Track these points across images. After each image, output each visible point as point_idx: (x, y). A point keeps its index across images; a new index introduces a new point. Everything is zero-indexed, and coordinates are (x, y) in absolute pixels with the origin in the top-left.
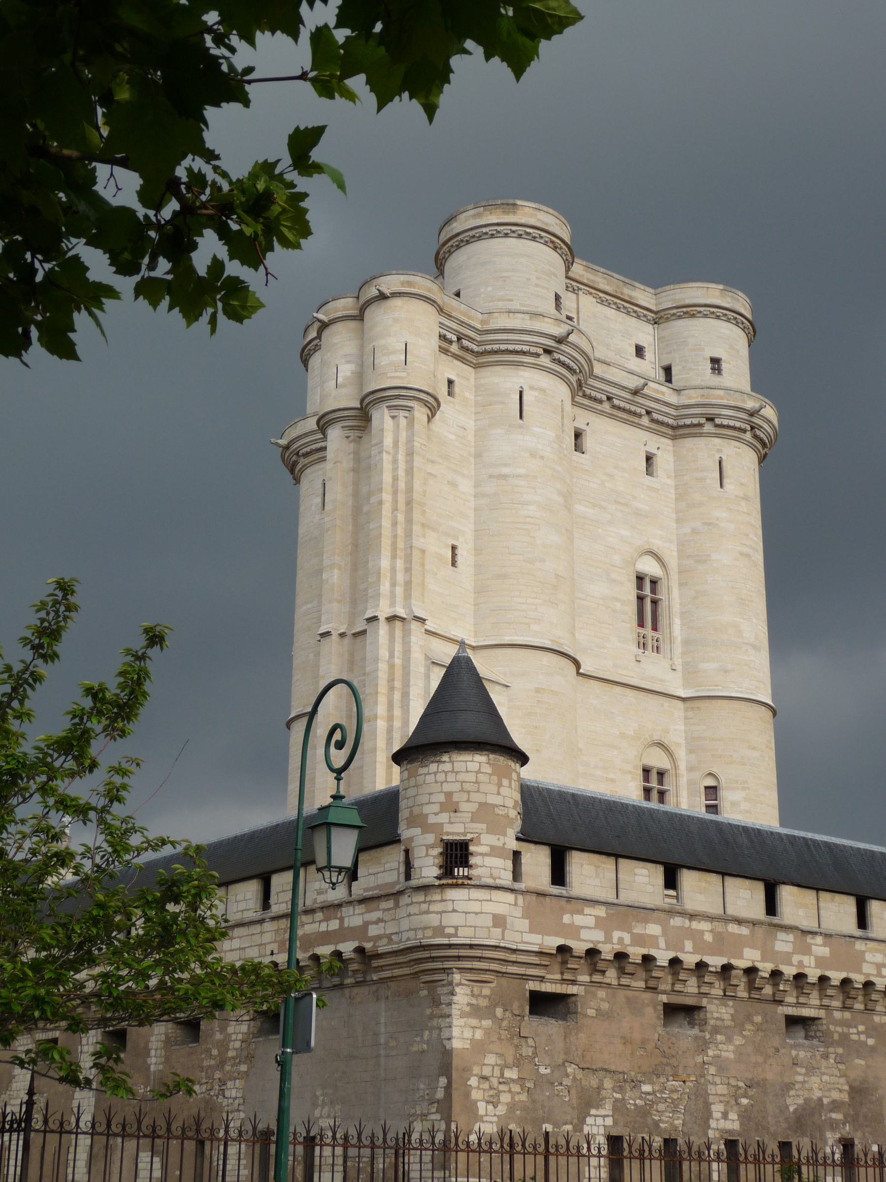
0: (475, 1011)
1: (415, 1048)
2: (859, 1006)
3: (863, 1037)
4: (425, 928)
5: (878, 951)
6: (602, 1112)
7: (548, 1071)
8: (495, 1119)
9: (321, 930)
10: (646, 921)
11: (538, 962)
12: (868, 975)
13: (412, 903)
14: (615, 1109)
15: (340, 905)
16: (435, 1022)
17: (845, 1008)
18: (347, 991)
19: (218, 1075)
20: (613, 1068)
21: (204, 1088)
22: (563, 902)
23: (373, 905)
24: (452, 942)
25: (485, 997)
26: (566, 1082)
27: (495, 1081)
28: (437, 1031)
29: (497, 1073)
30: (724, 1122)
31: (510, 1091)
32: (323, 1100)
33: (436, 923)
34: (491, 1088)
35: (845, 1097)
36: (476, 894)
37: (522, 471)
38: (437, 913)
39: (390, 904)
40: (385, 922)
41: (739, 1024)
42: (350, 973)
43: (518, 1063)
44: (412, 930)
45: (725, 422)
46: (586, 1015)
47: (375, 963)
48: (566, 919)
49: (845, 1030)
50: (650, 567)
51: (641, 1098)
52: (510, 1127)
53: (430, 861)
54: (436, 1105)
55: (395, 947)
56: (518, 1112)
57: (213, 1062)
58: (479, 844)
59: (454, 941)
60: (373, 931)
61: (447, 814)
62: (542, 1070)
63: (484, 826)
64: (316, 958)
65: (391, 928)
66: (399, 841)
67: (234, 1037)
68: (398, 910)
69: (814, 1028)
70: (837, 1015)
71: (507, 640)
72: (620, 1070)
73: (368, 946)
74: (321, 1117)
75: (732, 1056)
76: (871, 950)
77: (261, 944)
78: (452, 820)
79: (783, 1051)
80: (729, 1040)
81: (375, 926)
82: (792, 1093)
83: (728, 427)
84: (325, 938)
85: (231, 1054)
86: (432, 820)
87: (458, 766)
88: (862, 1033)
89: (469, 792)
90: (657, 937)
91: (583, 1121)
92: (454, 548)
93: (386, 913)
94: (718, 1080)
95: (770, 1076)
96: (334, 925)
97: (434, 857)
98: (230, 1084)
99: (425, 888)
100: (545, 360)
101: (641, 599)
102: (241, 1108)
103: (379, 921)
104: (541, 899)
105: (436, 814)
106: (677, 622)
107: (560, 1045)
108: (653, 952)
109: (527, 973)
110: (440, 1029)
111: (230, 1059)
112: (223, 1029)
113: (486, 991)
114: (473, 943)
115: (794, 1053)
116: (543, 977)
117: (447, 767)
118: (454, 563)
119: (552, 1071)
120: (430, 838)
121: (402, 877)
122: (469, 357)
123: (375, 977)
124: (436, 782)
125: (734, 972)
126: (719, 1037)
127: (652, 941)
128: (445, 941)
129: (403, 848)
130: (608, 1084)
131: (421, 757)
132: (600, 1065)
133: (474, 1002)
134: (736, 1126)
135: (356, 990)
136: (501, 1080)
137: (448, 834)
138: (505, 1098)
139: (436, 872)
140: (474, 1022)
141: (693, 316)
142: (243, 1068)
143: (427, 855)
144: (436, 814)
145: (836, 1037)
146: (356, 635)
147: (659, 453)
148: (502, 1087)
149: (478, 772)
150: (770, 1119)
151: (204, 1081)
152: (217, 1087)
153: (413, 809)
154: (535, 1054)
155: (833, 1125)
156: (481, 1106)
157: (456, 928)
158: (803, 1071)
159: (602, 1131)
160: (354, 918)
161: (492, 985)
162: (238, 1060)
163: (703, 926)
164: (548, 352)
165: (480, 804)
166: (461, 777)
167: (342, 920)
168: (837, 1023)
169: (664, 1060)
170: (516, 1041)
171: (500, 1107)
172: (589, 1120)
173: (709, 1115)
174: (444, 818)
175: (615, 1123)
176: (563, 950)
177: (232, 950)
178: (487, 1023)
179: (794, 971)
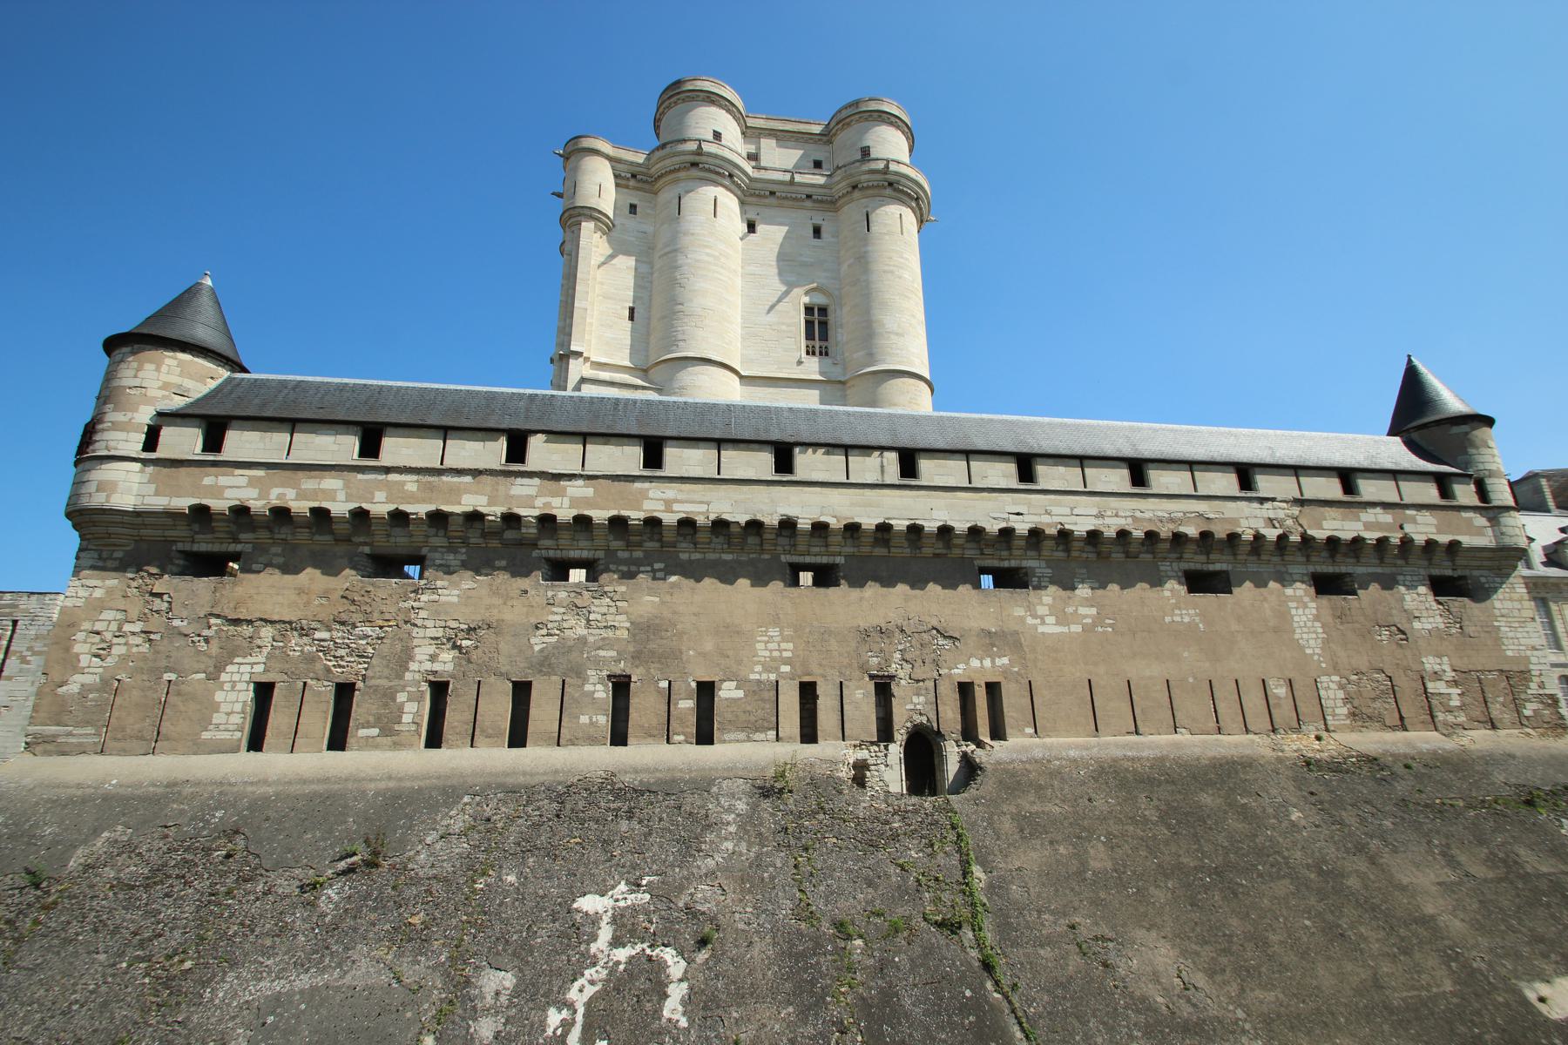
6: (250, 659)
10: (322, 478)
14: (269, 657)
20: (276, 618)
29: (114, 626)
34: (103, 641)
43: (142, 618)
48: (207, 481)
50: (820, 300)
62: (176, 623)
70: (622, 555)
82: (544, 632)
83: (868, 187)
90: (335, 491)
91: (220, 668)
94: (429, 623)
100: (694, 172)
101: (809, 324)
108: (325, 505)
115: (550, 594)
122: (646, 186)
127: (331, 495)
132: (258, 615)
134: (450, 667)
141: (848, 124)
148: (116, 640)
155: (598, 663)
156: (84, 660)
164: (695, 165)
169: (353, 608)
173: (411, 658)
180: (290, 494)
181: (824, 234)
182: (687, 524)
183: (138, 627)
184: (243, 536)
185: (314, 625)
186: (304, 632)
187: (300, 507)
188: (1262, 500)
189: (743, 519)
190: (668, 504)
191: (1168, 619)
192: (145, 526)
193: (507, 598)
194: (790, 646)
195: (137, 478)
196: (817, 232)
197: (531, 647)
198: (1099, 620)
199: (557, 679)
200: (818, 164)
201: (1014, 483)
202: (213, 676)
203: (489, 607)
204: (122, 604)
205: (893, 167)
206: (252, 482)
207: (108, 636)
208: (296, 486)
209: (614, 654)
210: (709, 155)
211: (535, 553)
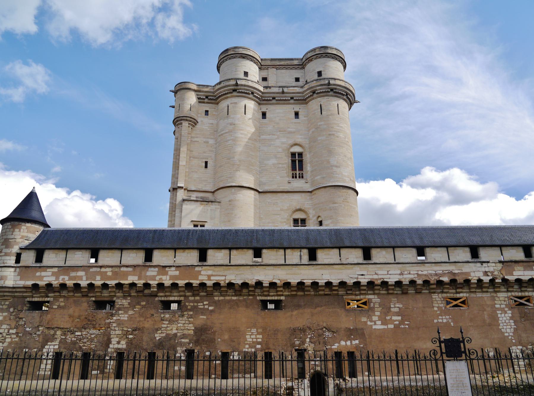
3: (206, 307)
5: (209, 270)
6: (53, 343)
10: (77, 271)
14: (60, 342)
17: (194, 295)
20: (62, 327)
26: (38, 333)
29: (6, 331)
31: (11, 338)
34: (2, 337)
37: (227, 131)
41: (132, 306)
43: (16, 327)
45: (319, 91)
48: (38, 274)
49: (195, 304)
51: (75, 337)
62: (28, 329)
70: (191, 298)
71: (221, 186)
72: (65, 327)
76: (205, 270)
80: (126, 312)
82: (160, 332)
83: (320, 93)
88: (206, 305)
90: (82, 276)
91: (43, 347)
92: (206, 163)
94: (117, 329)
100: (235, 94)
101: (293, 162)
104: (27, 268)
106: (309, 165)
107: (37, 319)
108: (79, 282)
113: (7, 303)
115: (162, 316)
118: (206, 167)
125: (124, 286)
126: (120, 312)
127: (81, 278)
130: (59, 333)
132: (55, 326)
134: (124, 346)
138: (8, 340)
141: (311, 60)
145: (189, 307)
147: (300, 110)
148: (7, 336)
150: (144, 343)
154: (25, 324)
155: (181, 345)
158: (167, 322)
164: (235, 90)
168: (191, 302)
169: (89, 323)
170: (17, 319)
171: (5, 344)
175: (59, 347)
179: (157, 282)
180: (66, 278)
181: (300, 116)
182: (217, 285)
183: (14, 331)
184: (50, 295)
185: (75, 330)
186: (73, 333)
187: (70, 283)
188: (482, 263)
189: (240, 282)
190: (209, 277)
191: (435, 321)
192: (16, 292)
193: (146, 318)
194: (261, 336)
195: (12, 274)
196: (297, 114)
197: (155, 338)
198: (402, 322)
200: (297, 80)
201: (361, 260)
203: (139, 321)
204: (8, 322)
205: (332, 82)
206: (53, 274)
207: (4, 335)
209: (187, 340)
210: (242, 85)
211: (157, 299)
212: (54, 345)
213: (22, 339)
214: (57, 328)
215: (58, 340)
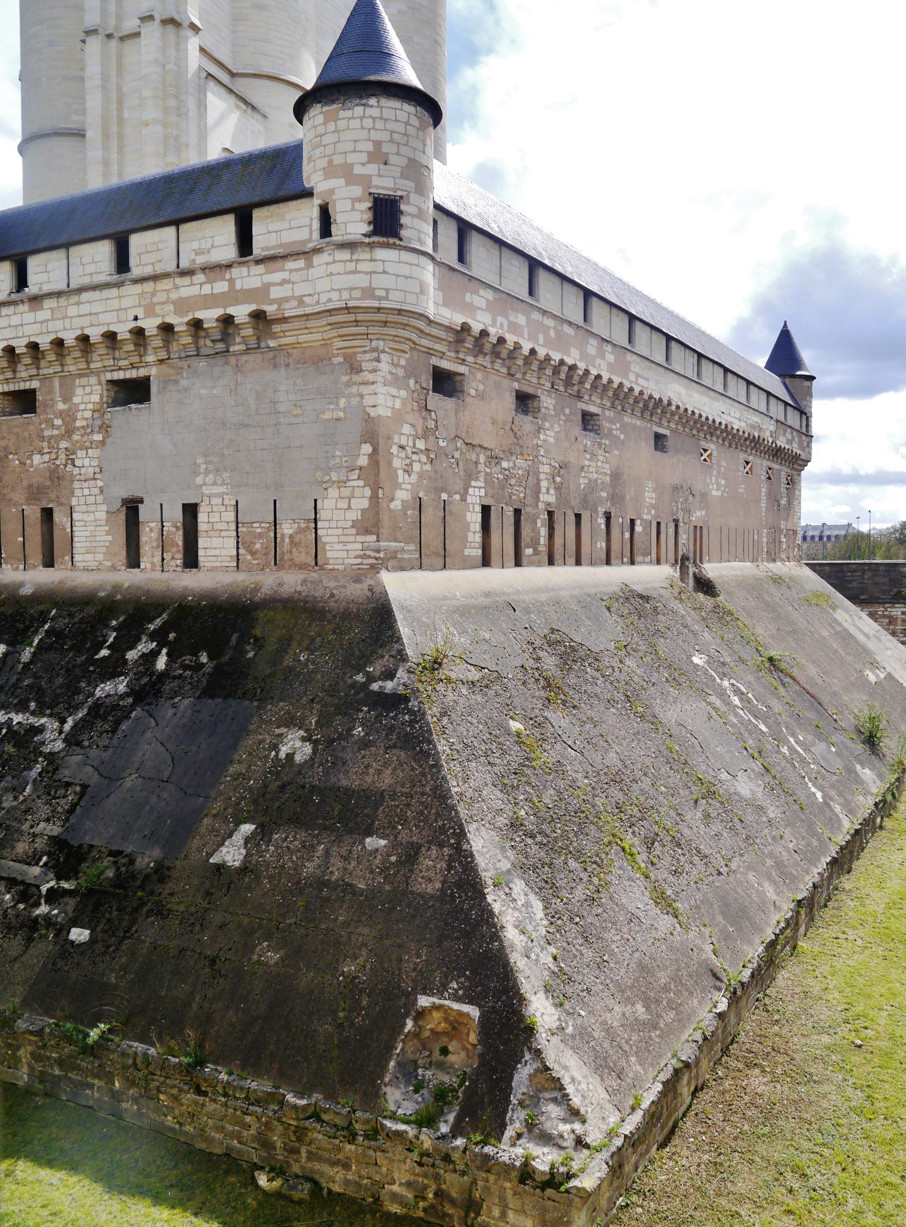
0: (396, 381)
1: (328, 415)
2: (619, 408)
4: (352, 289)
7: (445, 444)
8: (409, 487)
9: (203, 293)
11: (445, 337)
12: (631, 382)
13: (335, 262)
14: (486, 482)
15: (229, 266)
16: (354, 390)
18: (233, 360)
19: (63, 444)
20: (485, 445)
21: (46, 458)
22: (466, 279)
23: (280, 263)
24: (382, 305)
25: (402, 367)
27: (409, 450)
28: (358, 399)
29: (411, 444)
30: (548, 497)
31: (419, 461)
32: (206, 469)
33: (365, 284)
35: (608, 478)
36: (406, 256)
38: (366, 273)
39: (301, 263)
40: (294, 283)
42: (238, 340)
43: (426, 434)
44: (335, 290)
46: (469, 394)
47: (276, 328)
48: (468, 297)
52: (420, 495)
53: (357, 216)
54: (357, 472)
55: (308, 310)
56: (425, 482)
57: (56, 432)
58: (408, 203)
59: (384, 304)
60: (276, 293)
61: (376, 166)
63: (412, 184)
64: (197, 324)
65: (300, 290)
66: (308, 194)
67: (82, 407)
68: (311, 271)
69: (592, 422)
70: (607, 412)
73: (270, 309)
74: (205, 484)
75: (551, 440)
77: (120, 309)
78: (382, 173)
79: (579, 439)
81: (278, 287)
82: (583, 474)
84: (210, 301)
85: (78, 424)
86: (358, 170)
87: (388, 114)
89: (398, 144)
91: (466, 492)
93: (293, 274)
94: (544, 460)
95: (572, 460)
96: (221, 287)
97: (362, 212)
98: (80, 453)
99: (350, 246)
102: (97, 476)
103: (284, 282)
104: (452, 273)
105: (363, 164)
108: (521, 342)
109: (435, 347)
110: (362, 396)
111: (78, 429)
112: (67, 399)
114: (403, 308)
116: (444, 354)
117: (375, 112)
119: (448, 444)
120: (357, 191)
121: (316, 234)
123: (272, 343)
124: (363, 128)
126: (547, 424)
128: (375, 304)
129: (317, 201)
130: (482, 459)
131: (342, 99)
133: (394, 371)
135: (244, 358)
136: (414, 450)
137: (377, 187)
139: (366, 228)
140: (394, 391)
142: (98, 437)
143: (353, 209)
144: (363, 164)
146: (122, 39)
148: (415, 457)
149: (407, 123)
151: (46, 450)
152: (64, 456)
153: (333, 157)
157: (387, 290)
159: (478, 502)
160: (249, 277)
161: (407, 356)
162: (89, 430)
163: (549, 322)
165: (409, 159)
166: (391, 126)
167: (232, 281)
170: (424, 413)
172: (471, 491)
173: (538, 492)
174: (372, 169)
175: (486, 495)
176: (465, 328)
177: (79, 316)
178: (403, 393)
183: (420, 444)
189: (657, 396)
190: (638, 376)
194: (654, 495)
199: (589, 512)
202: (464, 499)
204: (410, 418)
208: (506, 316)
212: (480, 488)
213: (436, 467)
214: (480, 446)
215: (482, 474)
